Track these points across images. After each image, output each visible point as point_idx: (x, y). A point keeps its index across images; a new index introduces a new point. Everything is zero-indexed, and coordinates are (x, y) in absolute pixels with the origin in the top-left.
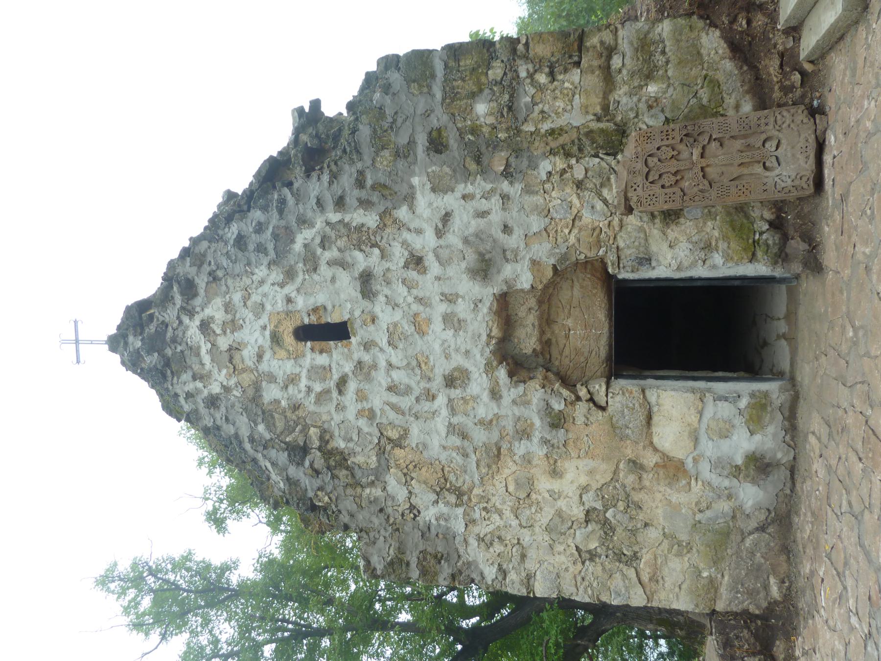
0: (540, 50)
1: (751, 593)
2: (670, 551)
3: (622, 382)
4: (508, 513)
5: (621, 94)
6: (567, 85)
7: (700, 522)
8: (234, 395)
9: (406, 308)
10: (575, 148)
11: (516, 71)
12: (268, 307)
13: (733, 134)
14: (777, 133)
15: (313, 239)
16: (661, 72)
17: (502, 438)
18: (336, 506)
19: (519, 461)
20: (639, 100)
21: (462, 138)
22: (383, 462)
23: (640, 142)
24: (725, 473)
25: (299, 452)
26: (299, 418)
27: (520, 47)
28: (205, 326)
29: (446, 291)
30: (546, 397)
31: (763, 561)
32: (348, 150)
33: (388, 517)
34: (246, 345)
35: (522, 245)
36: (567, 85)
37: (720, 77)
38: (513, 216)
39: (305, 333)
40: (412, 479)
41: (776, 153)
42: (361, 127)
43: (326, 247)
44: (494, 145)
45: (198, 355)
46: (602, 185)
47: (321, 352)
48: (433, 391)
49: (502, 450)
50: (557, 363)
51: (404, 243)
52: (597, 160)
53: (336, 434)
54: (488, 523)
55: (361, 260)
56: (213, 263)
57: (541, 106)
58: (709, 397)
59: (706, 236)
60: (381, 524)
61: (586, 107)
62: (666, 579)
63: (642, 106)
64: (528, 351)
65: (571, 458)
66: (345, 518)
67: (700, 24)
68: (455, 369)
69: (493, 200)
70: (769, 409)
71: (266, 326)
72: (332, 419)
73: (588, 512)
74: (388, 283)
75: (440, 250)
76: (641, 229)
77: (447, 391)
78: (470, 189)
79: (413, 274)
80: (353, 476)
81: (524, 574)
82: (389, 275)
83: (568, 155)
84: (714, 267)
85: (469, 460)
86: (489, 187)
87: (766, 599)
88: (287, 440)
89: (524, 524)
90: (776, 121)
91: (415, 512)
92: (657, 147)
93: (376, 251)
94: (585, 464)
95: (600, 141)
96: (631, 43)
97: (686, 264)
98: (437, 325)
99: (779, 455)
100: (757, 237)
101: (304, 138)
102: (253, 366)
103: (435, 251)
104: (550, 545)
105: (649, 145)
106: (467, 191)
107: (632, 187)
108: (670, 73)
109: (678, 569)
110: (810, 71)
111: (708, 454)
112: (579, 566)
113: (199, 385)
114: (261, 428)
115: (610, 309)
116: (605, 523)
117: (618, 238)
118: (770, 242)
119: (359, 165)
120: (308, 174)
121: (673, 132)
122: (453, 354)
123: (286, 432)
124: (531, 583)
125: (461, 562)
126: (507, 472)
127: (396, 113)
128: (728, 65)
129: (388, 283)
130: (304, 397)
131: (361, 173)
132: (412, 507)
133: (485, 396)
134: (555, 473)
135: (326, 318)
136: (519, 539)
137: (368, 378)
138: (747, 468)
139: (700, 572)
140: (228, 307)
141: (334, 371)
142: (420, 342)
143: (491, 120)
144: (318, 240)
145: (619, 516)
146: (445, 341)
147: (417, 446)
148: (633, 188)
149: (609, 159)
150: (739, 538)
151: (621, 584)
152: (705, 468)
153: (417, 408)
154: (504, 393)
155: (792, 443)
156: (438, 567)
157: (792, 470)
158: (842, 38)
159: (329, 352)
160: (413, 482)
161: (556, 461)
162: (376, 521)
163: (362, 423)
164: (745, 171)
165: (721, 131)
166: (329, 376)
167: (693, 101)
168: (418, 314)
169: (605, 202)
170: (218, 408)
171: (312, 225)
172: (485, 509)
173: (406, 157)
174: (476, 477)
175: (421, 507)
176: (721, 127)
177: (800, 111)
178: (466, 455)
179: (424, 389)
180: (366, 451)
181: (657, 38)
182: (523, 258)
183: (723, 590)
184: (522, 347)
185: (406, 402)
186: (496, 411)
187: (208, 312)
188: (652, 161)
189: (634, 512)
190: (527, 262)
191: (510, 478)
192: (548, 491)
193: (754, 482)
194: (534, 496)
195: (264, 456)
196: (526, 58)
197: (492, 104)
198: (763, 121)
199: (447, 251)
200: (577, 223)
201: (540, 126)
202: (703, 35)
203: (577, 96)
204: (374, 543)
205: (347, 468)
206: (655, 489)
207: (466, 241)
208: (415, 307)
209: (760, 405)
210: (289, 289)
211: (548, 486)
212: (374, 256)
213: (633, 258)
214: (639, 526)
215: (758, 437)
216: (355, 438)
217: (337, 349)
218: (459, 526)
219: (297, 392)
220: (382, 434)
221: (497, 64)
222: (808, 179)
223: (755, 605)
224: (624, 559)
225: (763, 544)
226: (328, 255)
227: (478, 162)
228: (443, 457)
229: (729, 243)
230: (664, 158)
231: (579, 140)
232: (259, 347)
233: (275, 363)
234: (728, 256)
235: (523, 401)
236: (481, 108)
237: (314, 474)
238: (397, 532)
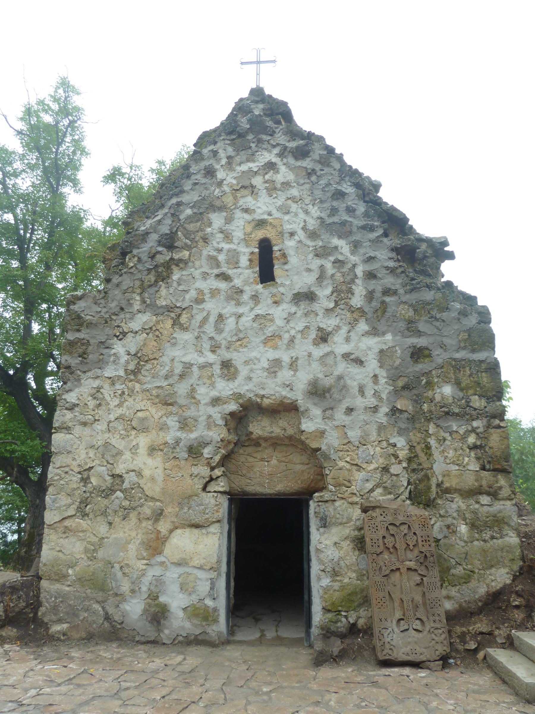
0: (495, 438)
1: (55, 609)
2: (89, 543)
3: (226, 504)
4: (119, 411)
6: (467, 459)
7: (112, 567)
8: (215, 190)
9: (286, 329)
10: (415, 466)
11: (477, 418)
12: (286, 217)
13: (427, 594)
14: (428, 630)
15: (341, 254)
16: (476, 535)
17: (181, 407)
18: (125, 273)
19: (162, 420)
20: (454, 518)
21: (423, 375)
22: (161, 310)
23: (420, 519)
24: (152, 588)
26: (196, 242)
27: (497, 422)
28: (271, 166)
29: (300, 362)
30: (214, 443)
31: (81, 618)
32: (414, 282)
33: (117, 315)
34: (256, 199)
35: (336, 423)
36: (467, 459)
37: (473, 584)
38: (360, 416)
40: (147, 334)
41: (411, 629)
42: (432, 292)
43: (335, 265)
44: (418, 401)
45: (248, 161)
46: (385, 488)
47: (250, 260)
48: (219, 351)
49: (171, 407)
50: (241, 451)
51: (338, 328)
52: (405, 484)
53: (184, 273)
54: (112, 396)
56: (322, 172)
57: (449, 438)
58: (213, 575)
59: (344, 573)
60: (111, 309)
61: (448, 475)
62: (67, 540)
63: (449, 521)
64: (251, 428)
65: (164, 463)
66: (116, 279)
67: (516, 568)
68: (236, 369)
69: (373, 399)
70: (204, 623)
71: (271, 215)
72: (196, 269)
73: (121, 476)
74: (306, 315)
75: (332, 357)
76: (349, 520)
77: (219, 363)
78: (382, 381)
79: (313, 334)
80: (150, 286)
81: (70, 424)
82: (312, 315)
83: (410, 460)
84: (319, 579)
85: (163, 380)
86: (384, 396)
87: (50, 620)
88: (179, 233)
89: (111, 425)
90: (437, 629)
91: (121, 337)
92: (416, 532)
93: (332, 305)
94: (160, 474)
95: (421, 487)
96: (500, 511)
97: (321, 556)
98: (272, 354)
99: (167, 632)
100: (343, 613)
101: (424, 246)
102: (239, 205)
103: (332, 352)
104: (94, 446)
105: (417, 526)
106: (380, 378)
107: (384, 512)
108: (476, 543)
109: (74, 550)
110: (478, 656)
111: (168, 574)
112: (77, 469)
113: (224, 161)
114: (189, 212)
115: (284, 494)
116: (112, 491)
117: (343, 501)
118: (339, 624)
119: (401, 291)
120: (395, 250)
121: (428, 546)
122: (248, 367)
123: (185, 232)
124: (63, 430)
125: (80, 373)
126: (153, 411)
127: (443, 321)
128: (482, 590)
129: (306, 315)
130: (213, 246)
131: (395, 293)
132: (124, 334)
133: (214, 393)
134: (152, 450)
135: (278, 264)
136: (98, 420)
137: (229, 298)
138: (156, 605)
139: (72, 567)
140: (286, 185)
141: (235, 271)
142: (258, 340)
143: (438, 398)
144: (340, 258)
145: (117, 502)
146: (259, 360)
147: (174, 338)
148: (382, 513)
149: (407, 494)
150: (100, 599)
151: (63, 503)
152: (157, 571)
153: (205, 338)
154: (218, 409)
155: (177, 642)
156: (76, 355)
157: (154, 642)
158: (504, 682)
159: (250, 267)
160: (145, 335)
161: (162, 450)
162: (113, 305)
163: (193, 294)
164: (397, 604)
165: (429, 585)
166: (231, 266)
167: (453, 562)
168: (281, 339)
169: (372, 490)
170: (205, 177)
171: (353, 253)
173: (408, 329)
174: (149, 386)
175: (125, 342)
176: (432, 584)
177: (445, 648)
178: (166, 377)
179: (221, 344)
180: (170, 296)
181: (504, 533)
182: (326, 424)
183: (57, 586)
184: (255, 423)
185: (209, 328)
186: (203, 402)
187: (283, 169)
188: (404, 528)
189: (120, 514)
190: (323, 427)
191: (148, 413)
192: (137, 444)
193: (145, 611)
194: (133, 432)
195: (166, 214)
196: (489, 426)
197: (451, 398)
198: (437, 618)
199: (332, 363)
200: (355, 467)
201: (433, 437)
202: (507, 570)
203: (457, 468)
204: (95, 303)
205: (156, 281)
206: (140, 531)
207: (340, 378)
208: (286, 336)
210: (301, 235)
211: (142, 445)
212: (328, 303)
213: (326, 513)
214: (110, 518)
215: (181, 614)
216: (181, 288)
217: (253, 273)
218: (109, 372)
219: (217, 241)
220: (184, 309)
221: (483, 403)
222: (390, 655)
223: (46, 612)
224: (83, 505)
225: (95, 618)
226: (329, 265)
227: (404, 388)
228: (165, 359)
229: (338, 591)
230: (407, 538)
231: (422, 470)
232: (254, 210)
233: (241, 223)
234: (328, 590)
235: (210, 424)
236: (447, 390)
237: (151, 255)
238: (104, 322)
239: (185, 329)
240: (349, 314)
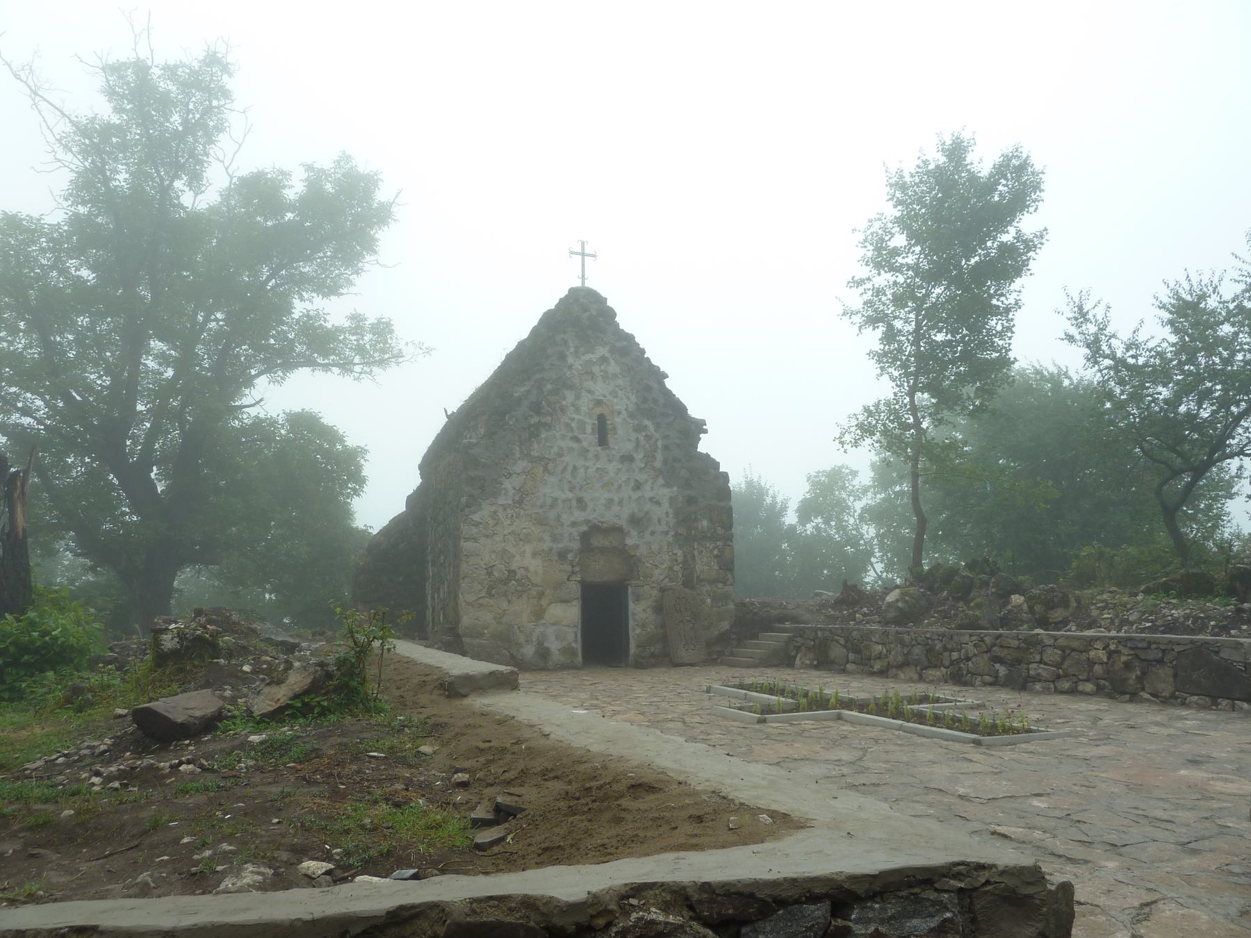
4: (511, 528)
5: (707, 588)
12: (615, 400)
25: (537, 408)
28: (604, 359)
39: (602, 419)
47: (592, 429)
51: (646, 481)
53: (549, 433)
55: (639, 456)
58: (576, 629)
78: (671, 516)
79: (632, 484)
84: (634, 630)
86: (671, 525)
93: (643, 466)
112: (485, 567)
113: (572, 350)
114: (549, 387)
126: (534, 528)
128: (716, 633)
132: (510, 475)
133: (572, 519)
134: (534, 554)
140: (615, 376)
143: (700, 527)
144: (649, 434)
152: (539, 629)
157: (544, 669)
158: (733, 666)
159: (592, 434)
163: (555, 449)
171: (656, 431)
172: (512, 516)
178: (541, 507)
185: (568, 475)
187: (612, 362)
190: (638, 543)
194: (521, 543)
207: (647, 513)
208: (616, 484)
209: (573, 653)
210: (624, 414)
215: (557, 653)
216: (548, 444)
218: (501, 501)
236: (705, 523)
239: (551, 474)
240: (653, 472)
